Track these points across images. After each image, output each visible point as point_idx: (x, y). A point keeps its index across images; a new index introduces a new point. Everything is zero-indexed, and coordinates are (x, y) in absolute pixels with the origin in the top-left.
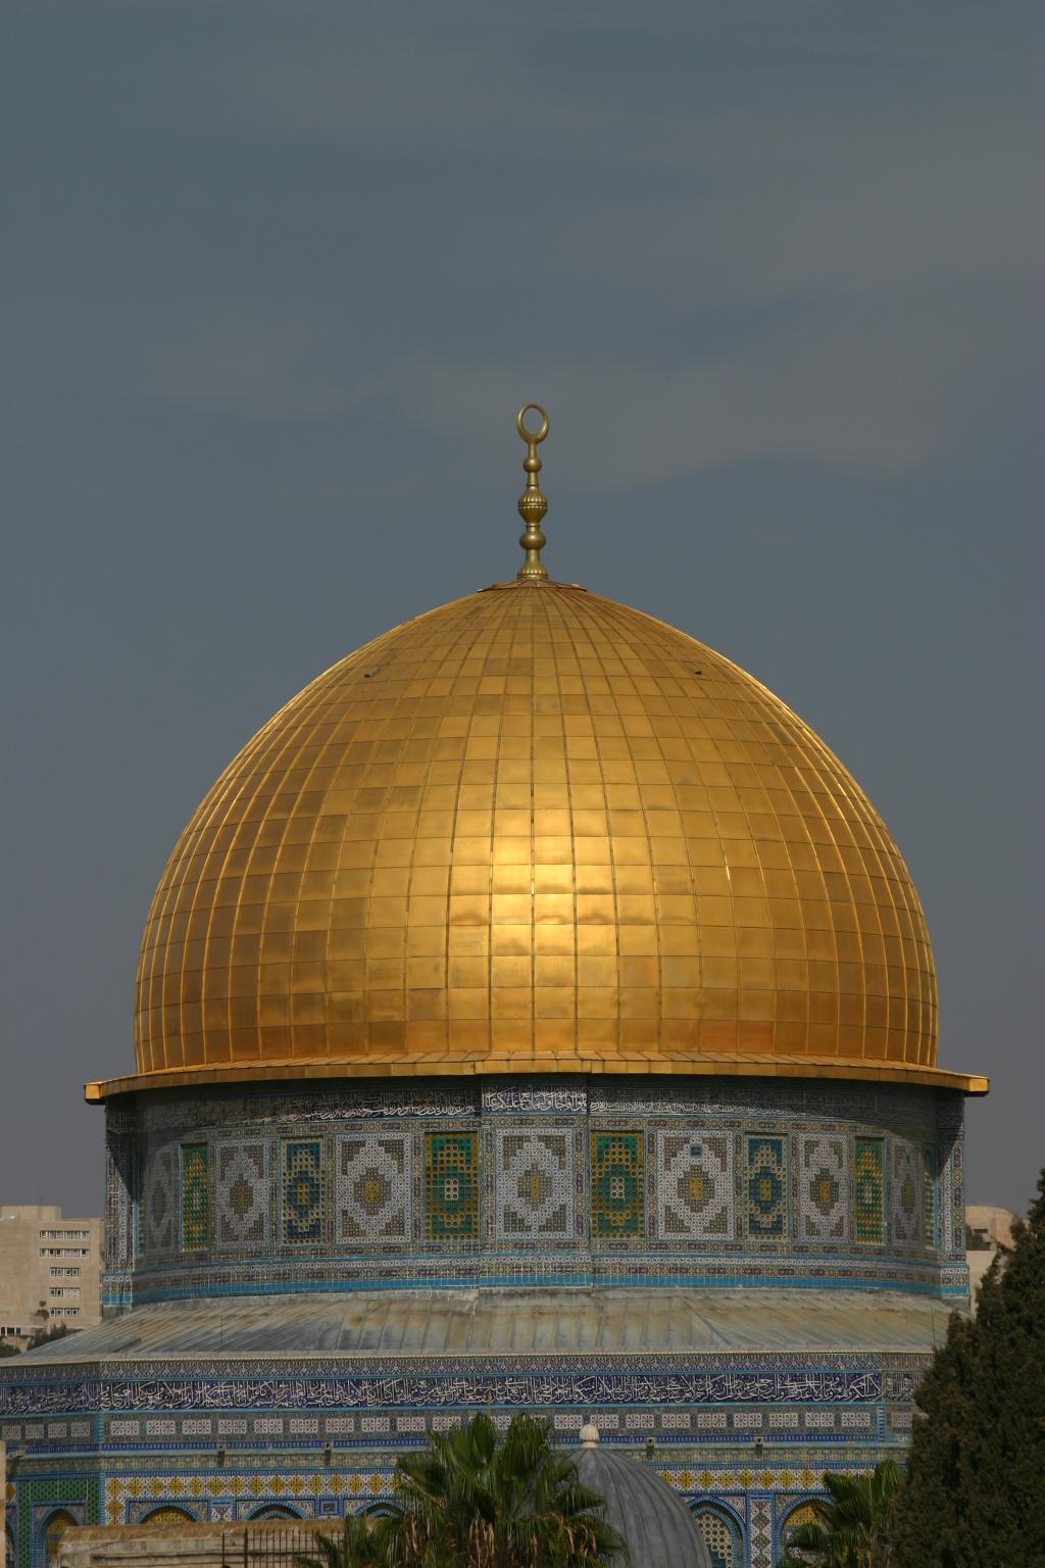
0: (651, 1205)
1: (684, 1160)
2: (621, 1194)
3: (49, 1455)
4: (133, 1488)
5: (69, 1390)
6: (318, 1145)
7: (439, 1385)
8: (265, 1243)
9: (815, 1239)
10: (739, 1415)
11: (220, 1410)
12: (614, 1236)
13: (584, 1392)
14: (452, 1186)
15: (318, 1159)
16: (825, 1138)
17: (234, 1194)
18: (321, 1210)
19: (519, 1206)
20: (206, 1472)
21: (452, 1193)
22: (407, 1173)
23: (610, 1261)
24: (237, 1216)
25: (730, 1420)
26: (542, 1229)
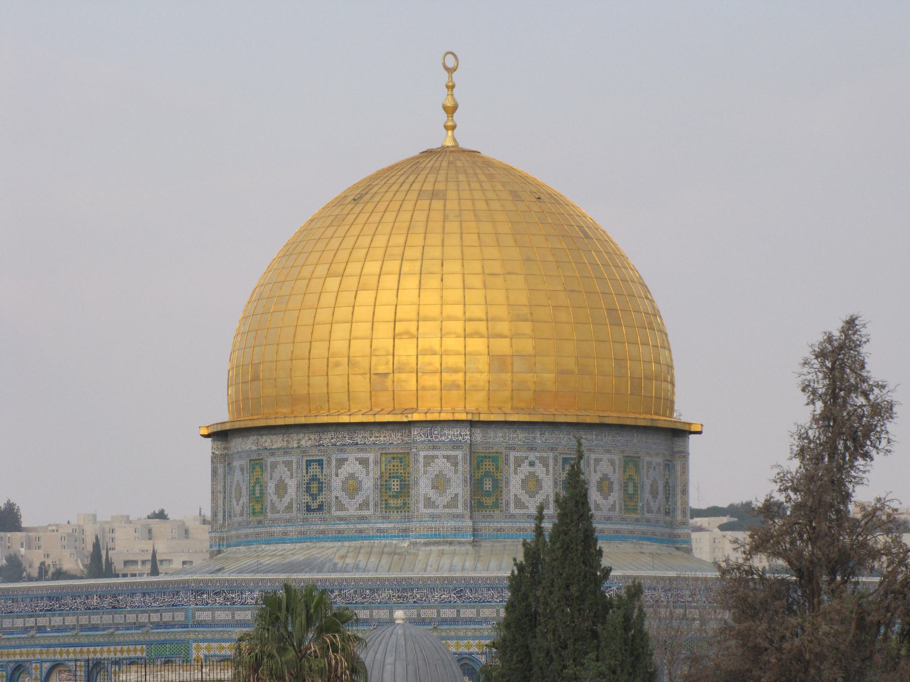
0: (507, 494)
1: (525, 469)
2: (489, 488)
3: (163, 630)
5: (173, 594)
6: (322, 460)
7: (377, 593)
12: (486, 511)
14: (396, 483)
15: (322, 468)
16: (606, 457)
17: (277, 487)
18: (324, 496)
19: (432, 494)
22: (371, 475)
23: (483, 525)
26: (444, 507)
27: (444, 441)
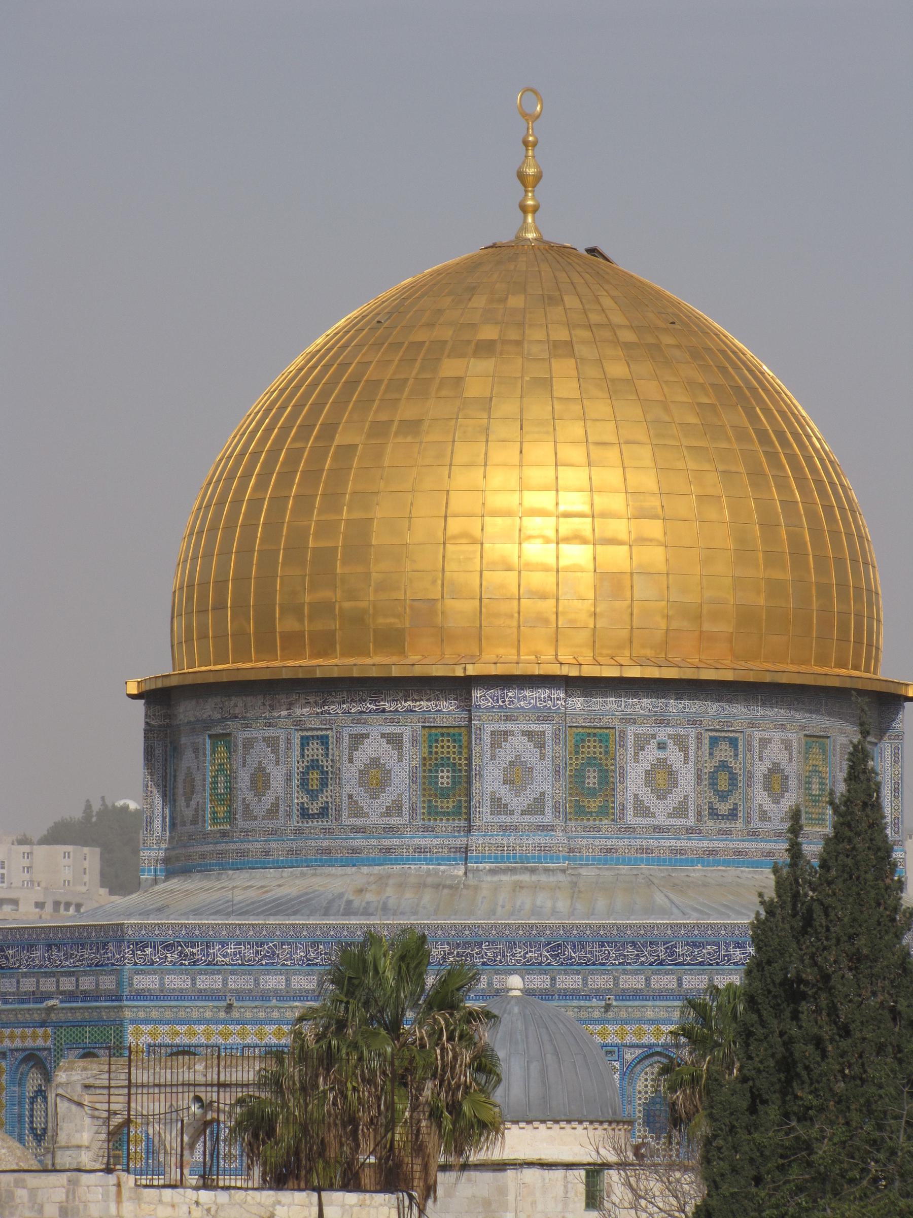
1: (651, 754)
3: (80, 1005)
4: (153, 1035)
5: (98, 947)
6: (327, 737)
8: (281, 821)
9: (767, 825)
10: (687, 977)
11: (230, 967)
13: (551, 955)
14: (445, 774)
15: (328, 749)
16: (777, 735)
19: (504, 792)
20: (217, 1022)
21: (445, 780)
23: (584, 842)
24: (257, 798)
25: (679, 980)
27: (522, 708)
